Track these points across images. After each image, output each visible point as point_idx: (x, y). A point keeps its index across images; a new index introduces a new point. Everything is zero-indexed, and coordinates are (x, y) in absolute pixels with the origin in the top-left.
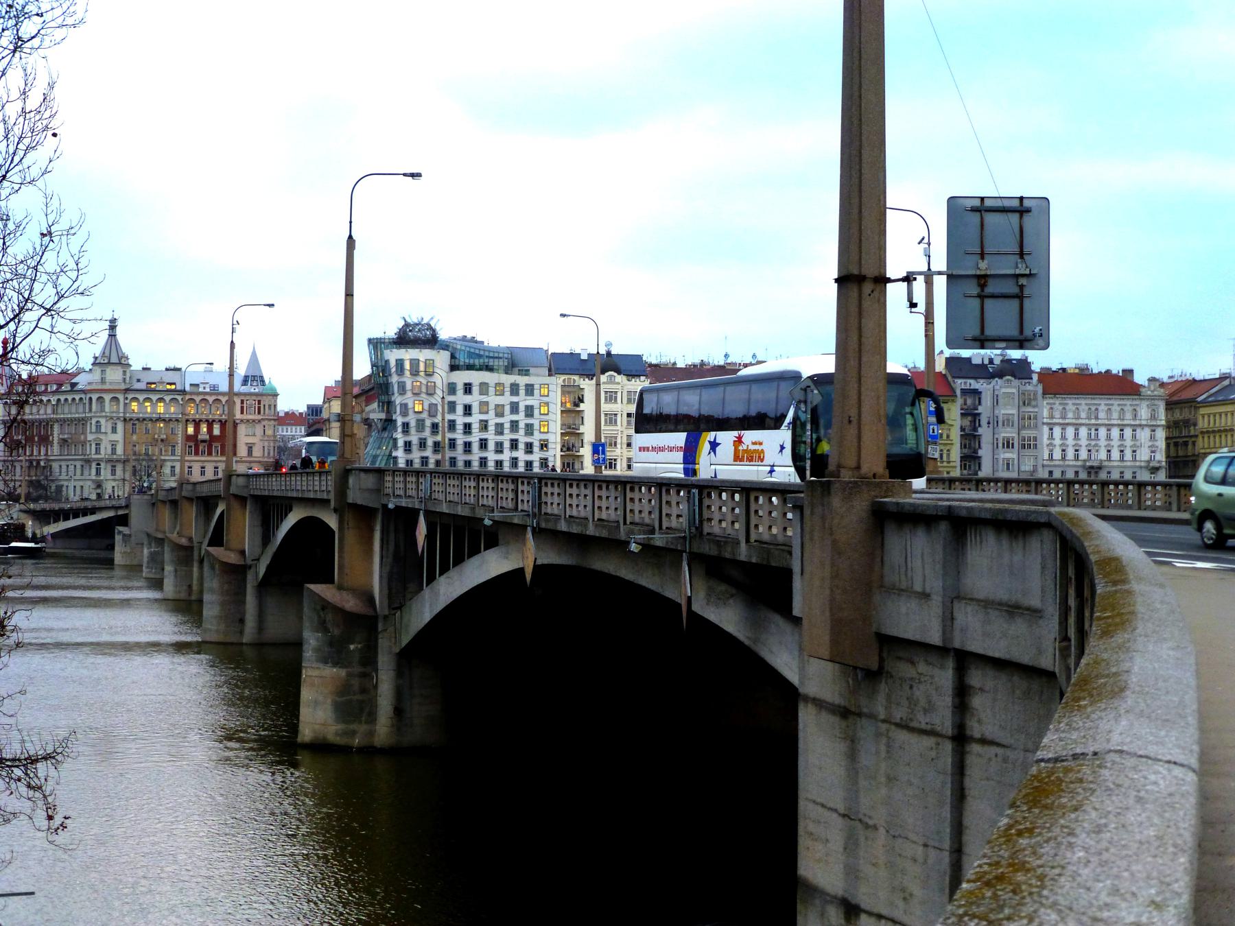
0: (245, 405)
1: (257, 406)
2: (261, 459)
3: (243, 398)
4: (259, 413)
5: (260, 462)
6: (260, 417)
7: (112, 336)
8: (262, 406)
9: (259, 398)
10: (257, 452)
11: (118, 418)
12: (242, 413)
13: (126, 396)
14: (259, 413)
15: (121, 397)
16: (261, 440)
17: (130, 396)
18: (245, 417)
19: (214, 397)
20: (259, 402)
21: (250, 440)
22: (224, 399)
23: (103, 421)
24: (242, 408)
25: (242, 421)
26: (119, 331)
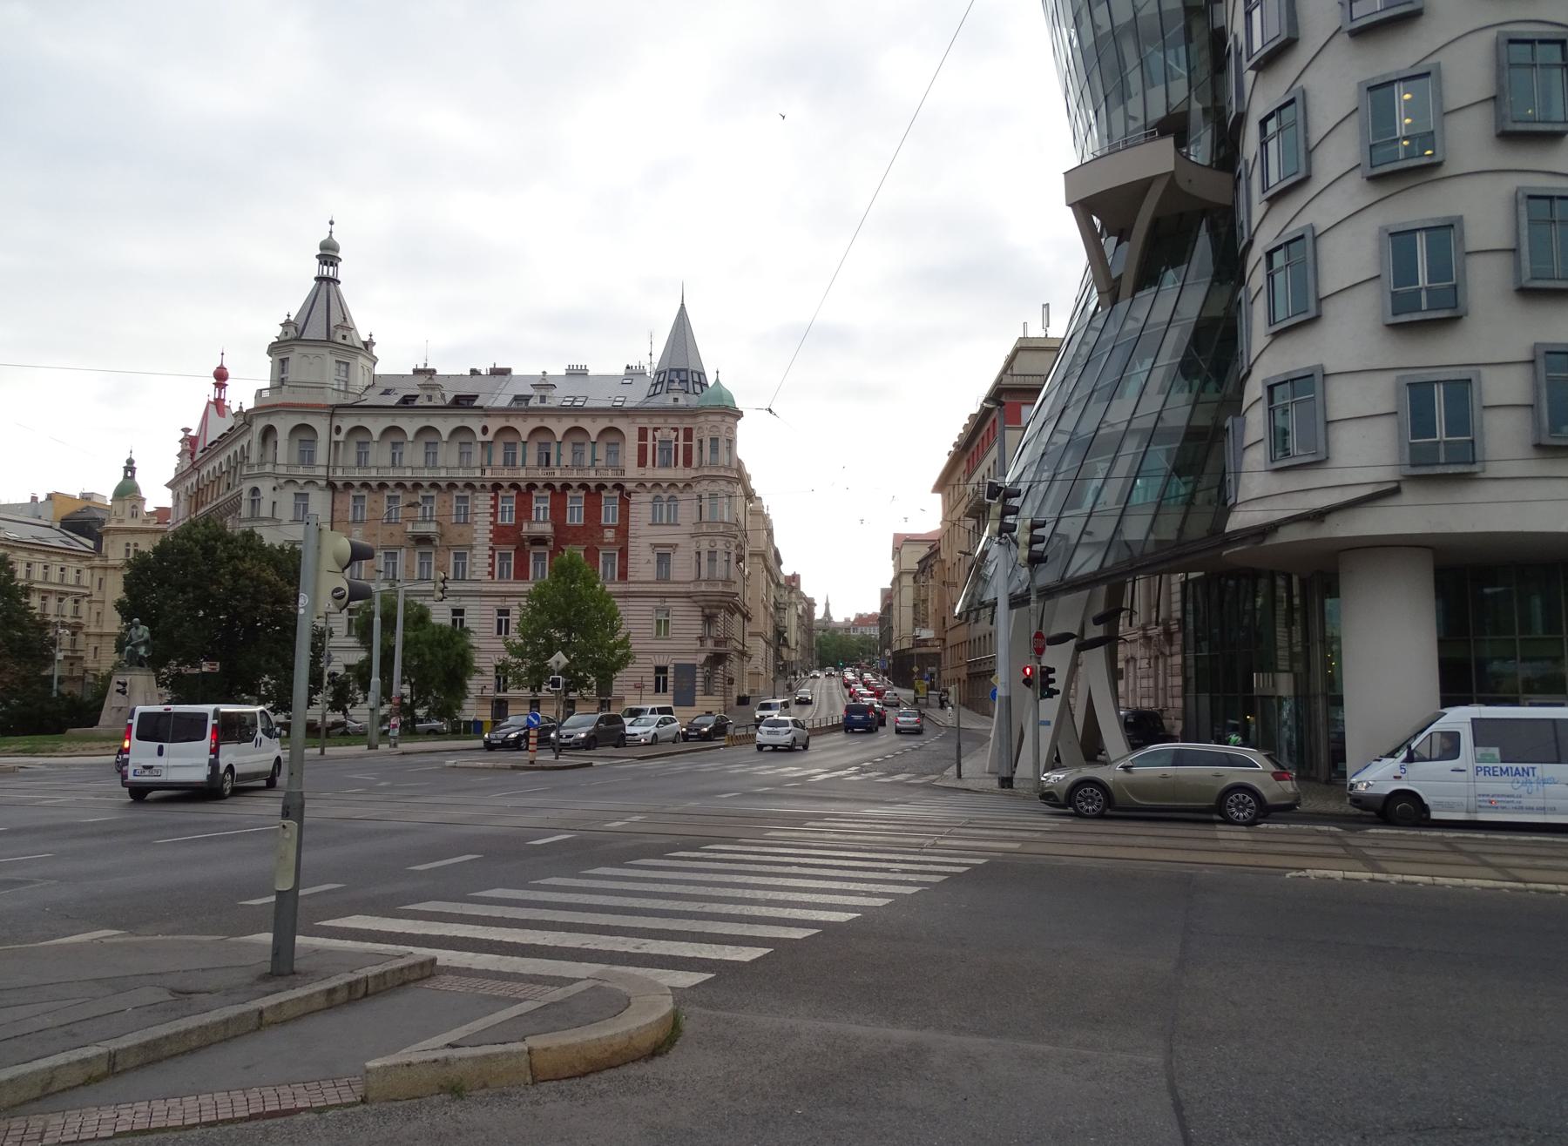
0: (650, 443)
1: (681, 443)
2: (692, 588)
3: (643, 422)
4: (688, 462)
5: (688, 595)
6: (690, 473)
7: (326, 283)
8: (695, 444)
9: (688, 423)
10: (682, 569)
11: (311, 482)
12: (642, 462)
13: (337, 422)
14: (688, 462)
15: (321, 425)
16: (693, 536)
17: (347, 424)
18: (650, 473)
19: (569, 423)
20: (688, 434)
21: (664, 535)
22: (594, 427)
23: (265, 487)
24: (642, 451)
25: (641, 485)
26: (344, 272)
